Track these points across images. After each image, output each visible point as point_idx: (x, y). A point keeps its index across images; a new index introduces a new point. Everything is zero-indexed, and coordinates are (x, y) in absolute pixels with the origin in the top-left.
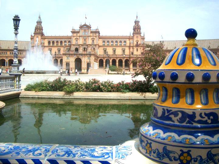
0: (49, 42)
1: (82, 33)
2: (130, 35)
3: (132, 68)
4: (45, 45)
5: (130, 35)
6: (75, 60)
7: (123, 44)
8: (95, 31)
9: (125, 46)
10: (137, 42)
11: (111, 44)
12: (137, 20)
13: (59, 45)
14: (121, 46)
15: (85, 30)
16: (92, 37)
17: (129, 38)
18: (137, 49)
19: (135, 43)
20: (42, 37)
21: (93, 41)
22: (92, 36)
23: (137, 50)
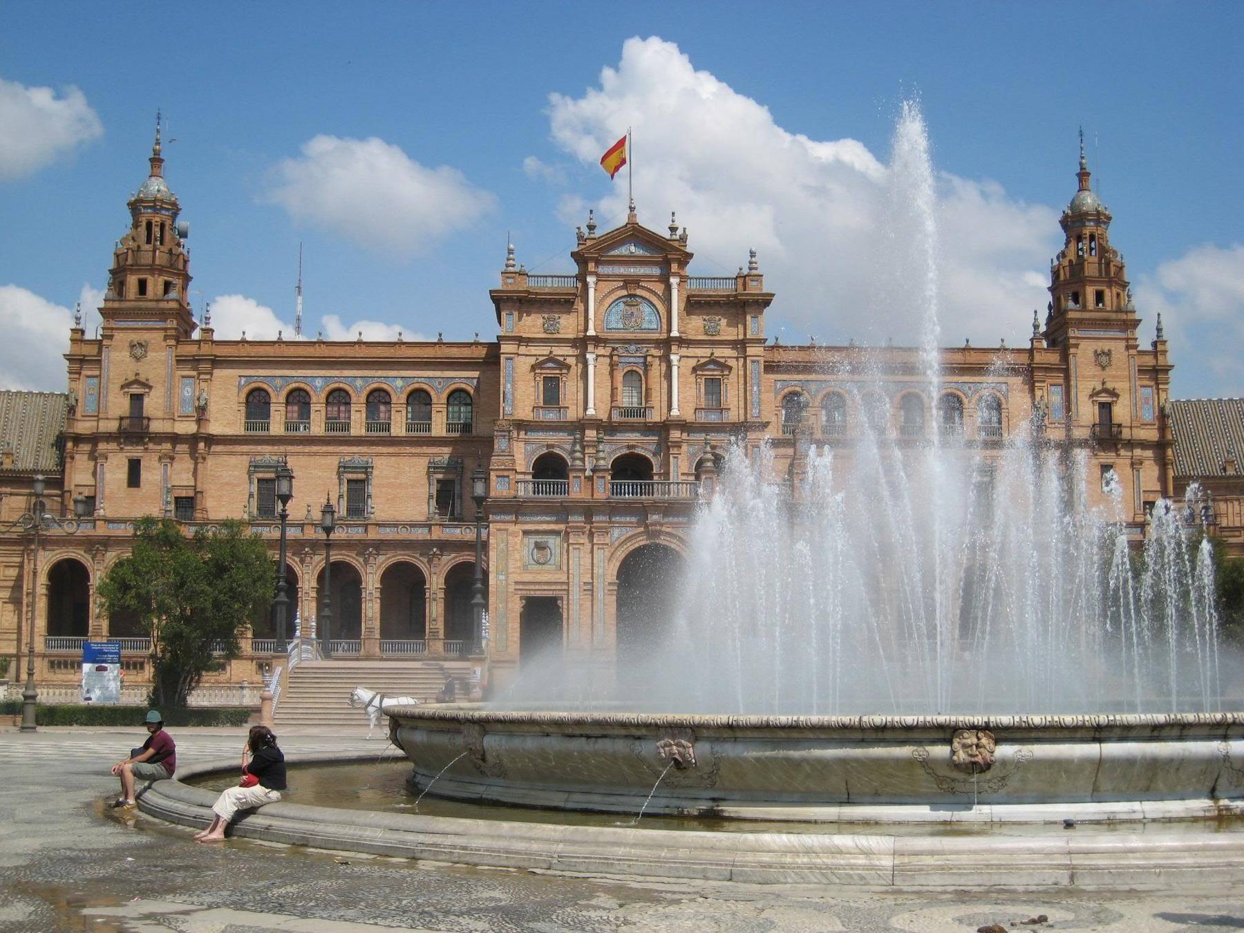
0: (257, 403)
1: (600, 309)
4: (214, 428)
6: (615, 565)
8: (727, 288)
10: (1106, 408)
12: (1089, 201)
13: (358, 424)
15: (629, 282)
16: (703, 352)
20: (190, 350)
21: (714, 386)
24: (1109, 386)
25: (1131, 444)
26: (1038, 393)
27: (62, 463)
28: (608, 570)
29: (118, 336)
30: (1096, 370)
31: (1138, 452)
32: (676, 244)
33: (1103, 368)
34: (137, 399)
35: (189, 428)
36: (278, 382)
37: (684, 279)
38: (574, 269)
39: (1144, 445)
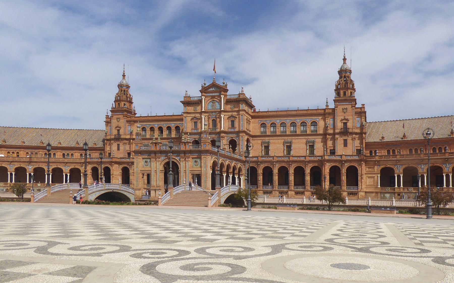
1: (206, 105)
2: (327, 106)
3: (309, 189)
5: (327, 106)
7: (310, 129)
9: (314, 133)
10: (345, 124)
11: (280, 130)
14: (304, 134)
15: (213, 97)
16: (230, 114)
17: (326, 113)
18: (345, 141)
19: (340, 125)
21: (233, 122)
22: (229, 112)
23: (345, 144)
24: (346, 118)
25: (352, 133)
26: (327, 120)
27: (104, 146)
28: (161, 168)
29: (114, 116)
30: (343, 114)
31: (354, 136)
32: (224, 87)
33: (345, 113)
34: (118, 130)
35: (128, 137)
36: (148, 126)
37: (225, 96)
38: (200, 94)
39: (356, 134)
